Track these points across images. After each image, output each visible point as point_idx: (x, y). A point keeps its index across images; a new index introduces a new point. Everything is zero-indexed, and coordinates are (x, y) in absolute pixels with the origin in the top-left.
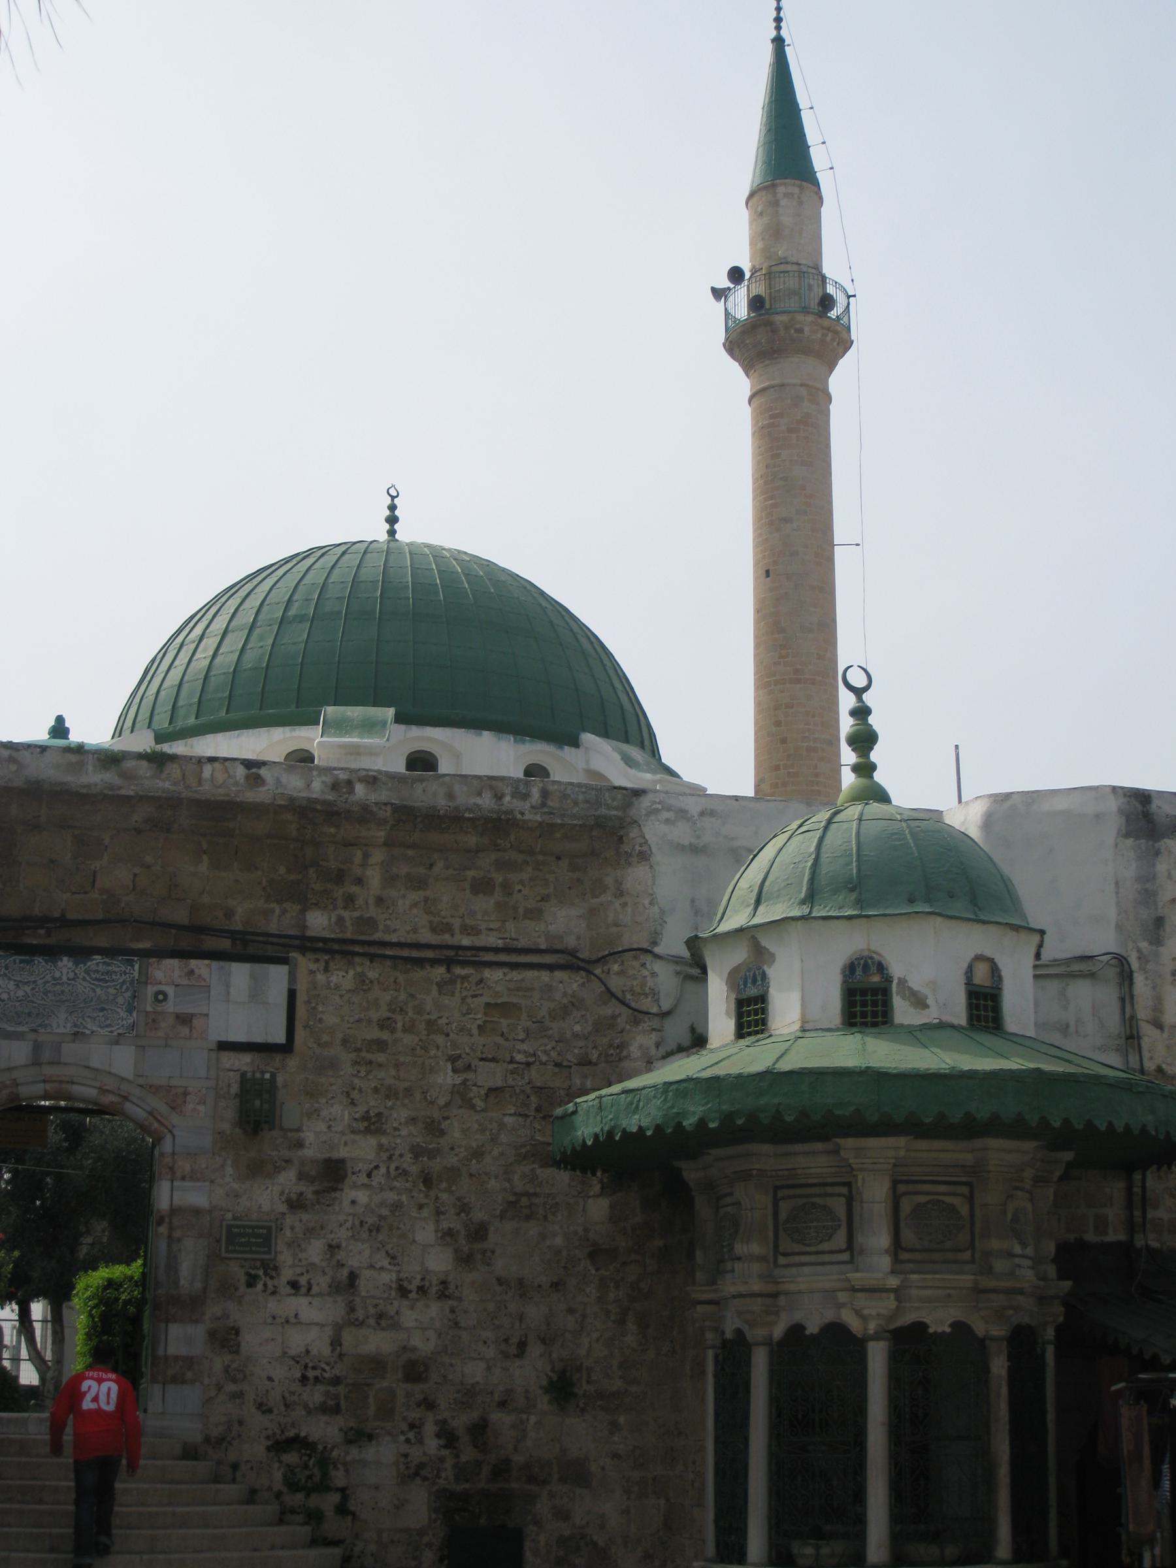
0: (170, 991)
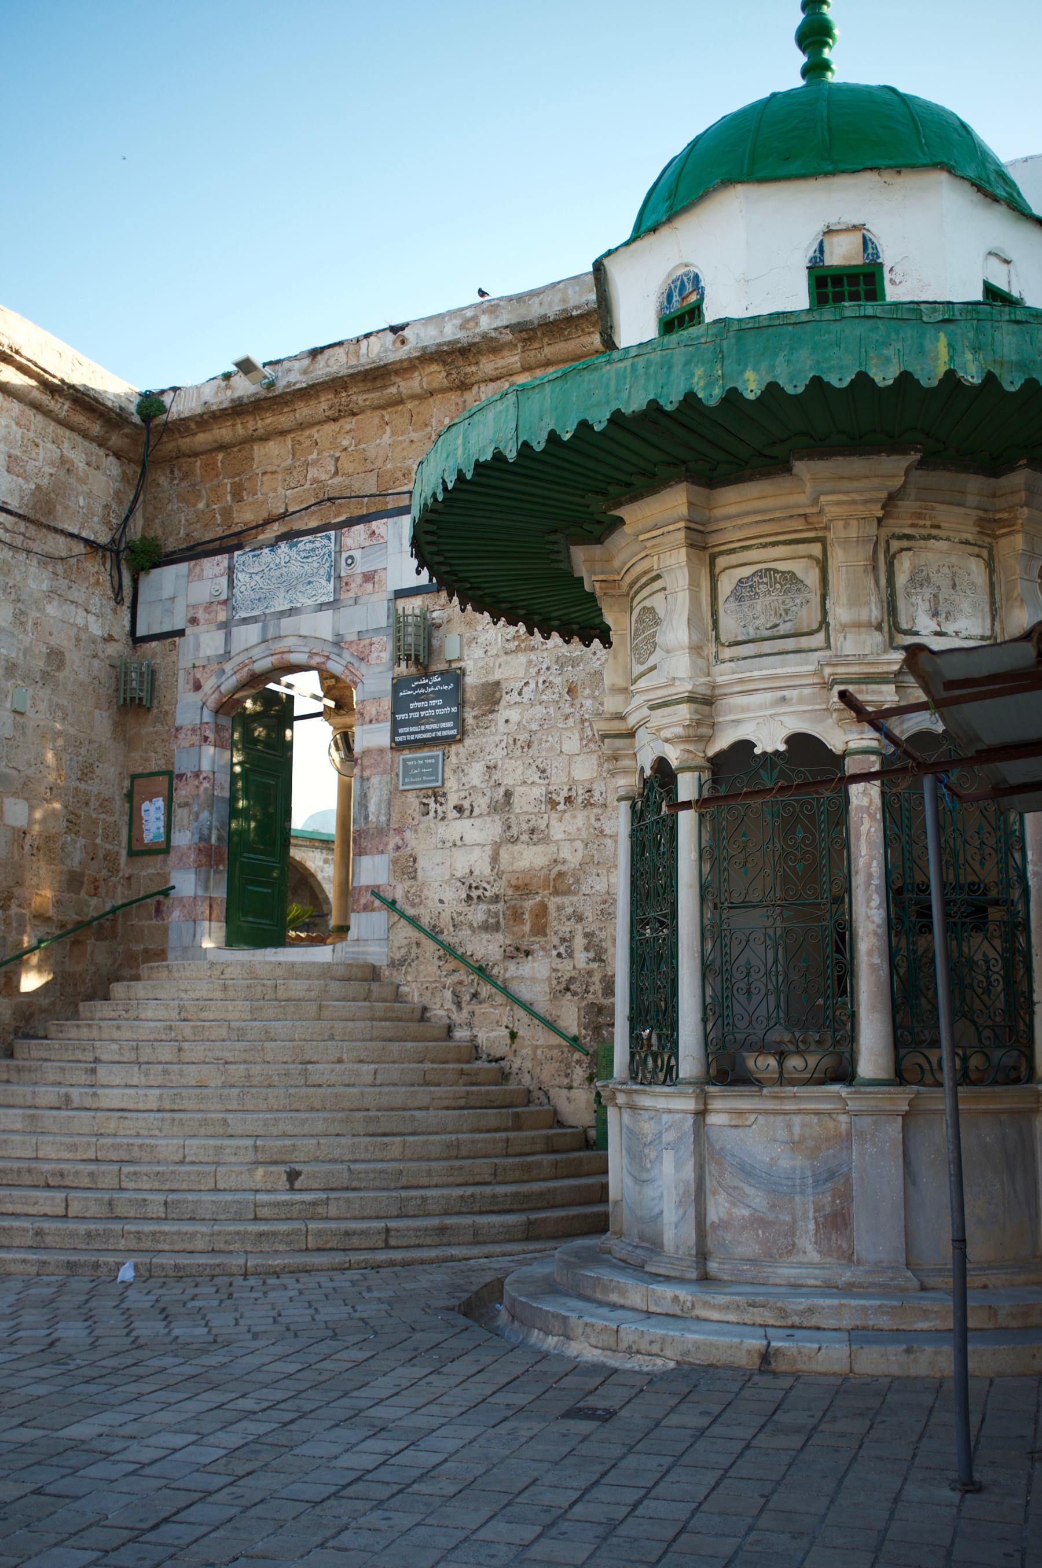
0: (357, 554)
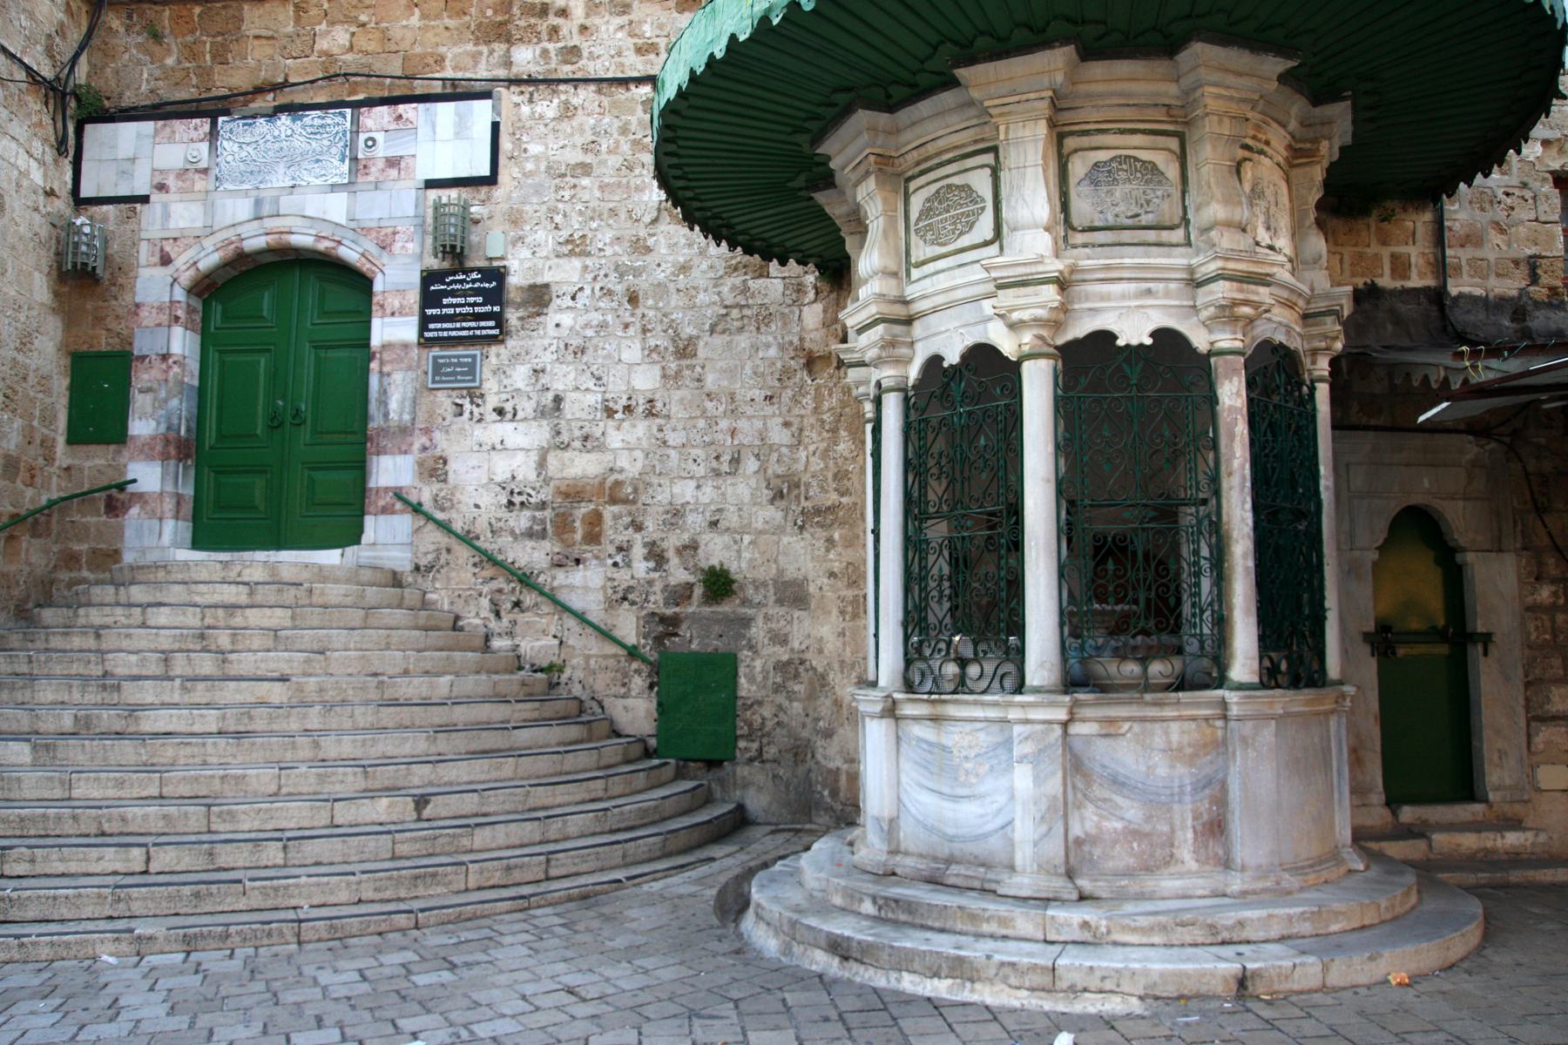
0: (379, 137)
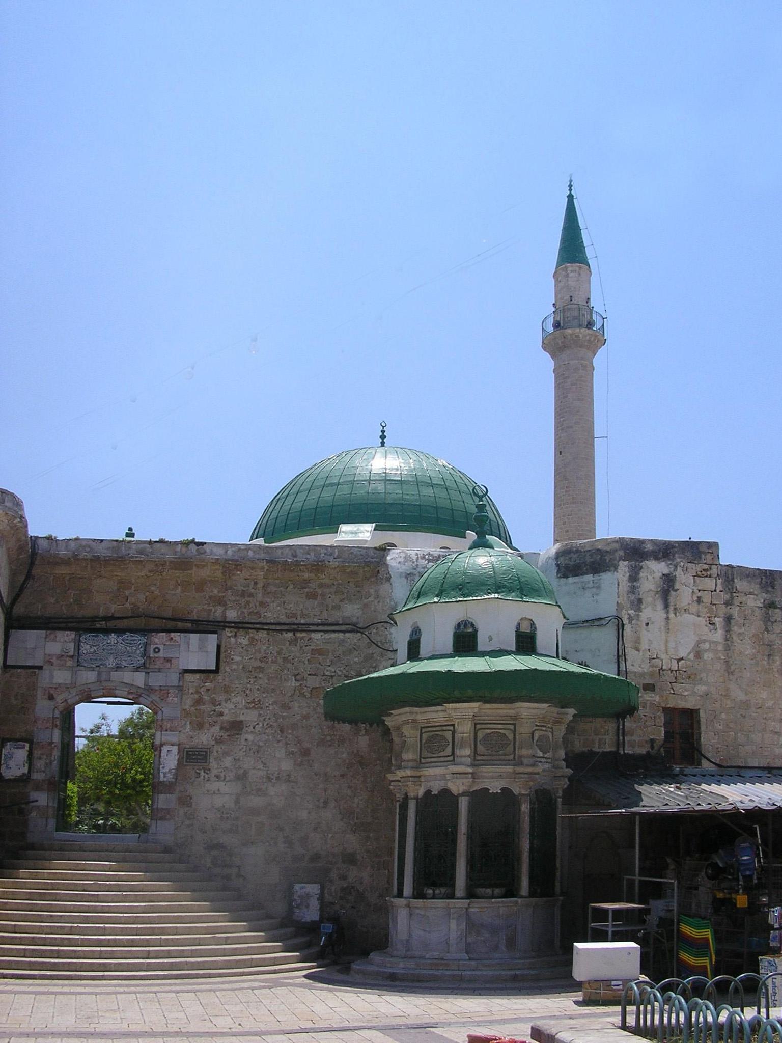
0: (162, 647)
